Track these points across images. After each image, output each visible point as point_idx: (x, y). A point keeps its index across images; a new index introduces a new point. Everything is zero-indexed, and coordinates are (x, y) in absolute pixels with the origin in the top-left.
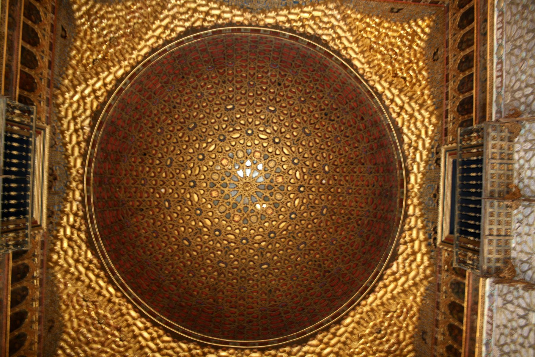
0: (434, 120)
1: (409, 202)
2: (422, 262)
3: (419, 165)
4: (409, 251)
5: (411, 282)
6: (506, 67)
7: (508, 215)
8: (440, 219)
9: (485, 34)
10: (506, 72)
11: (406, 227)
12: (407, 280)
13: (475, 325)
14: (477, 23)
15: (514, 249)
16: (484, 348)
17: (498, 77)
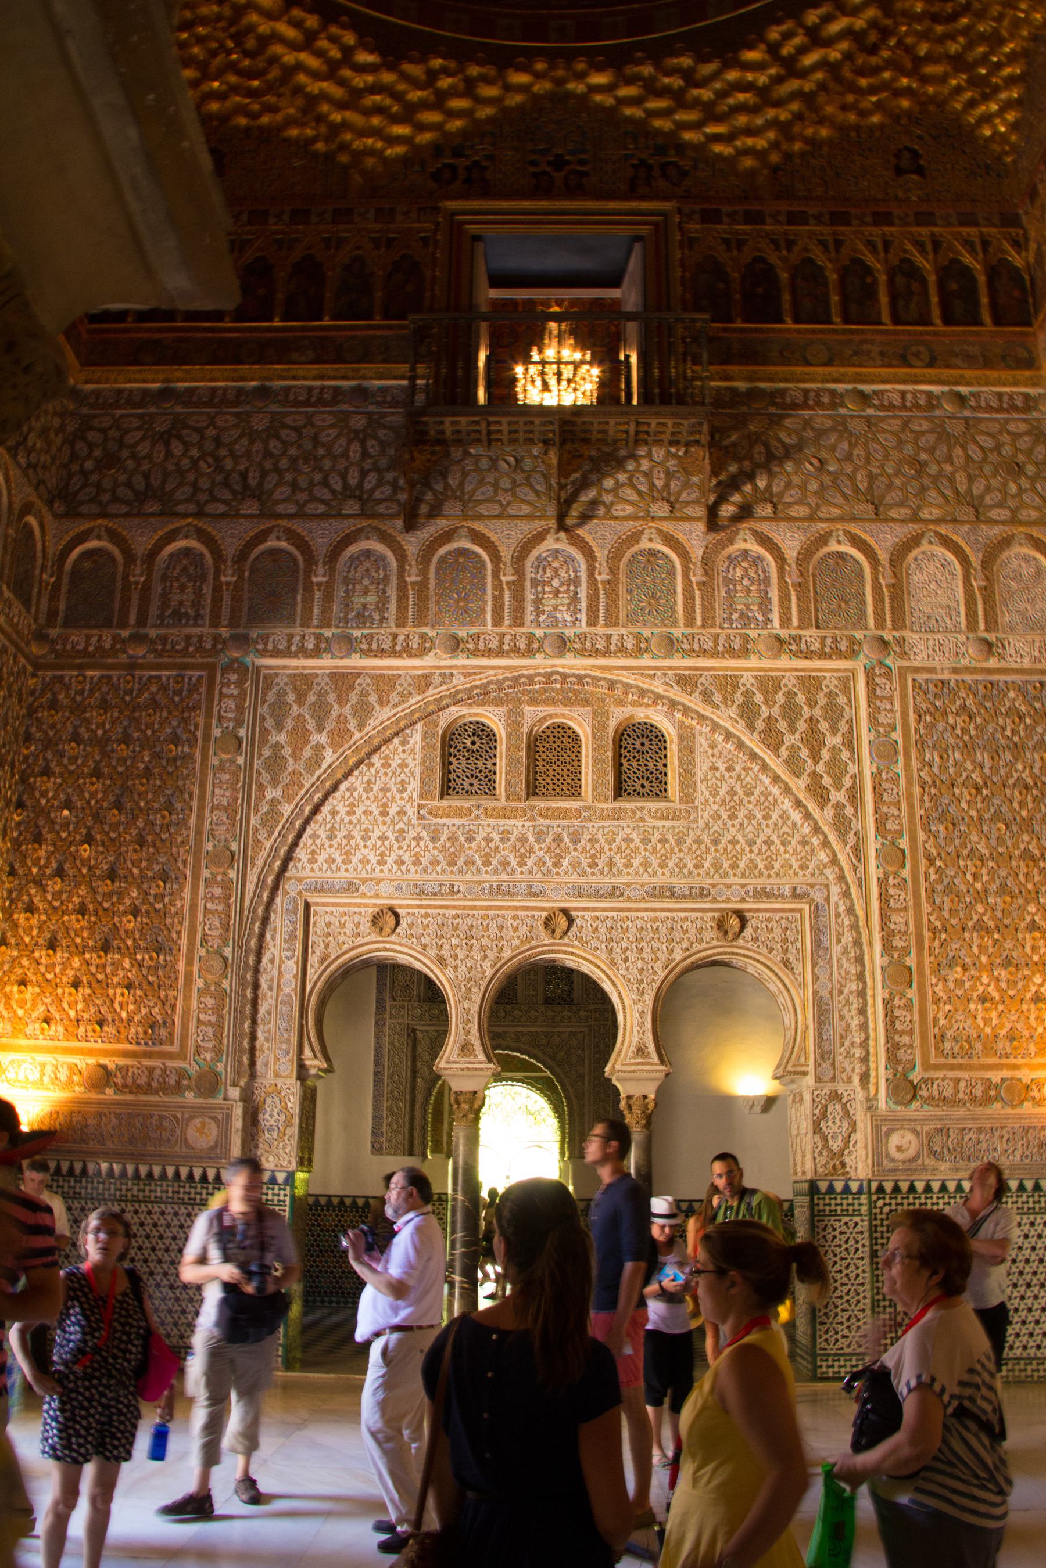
0: (748, 162)
1: (540, 66)
2: (393, 141)
3: (637, 101)
4: (415, 96)
5: (337, 117)
6: (821, 418)
7: (531, 442)
8: (505, 205)
9: (904, 360)
10: (811, 417)
11: (474, 71)
12: (341, 106)
13: (295, 356)
14: (935, 334)
15: (466, 454)
16: (254, 383)
17: (806, 392)
